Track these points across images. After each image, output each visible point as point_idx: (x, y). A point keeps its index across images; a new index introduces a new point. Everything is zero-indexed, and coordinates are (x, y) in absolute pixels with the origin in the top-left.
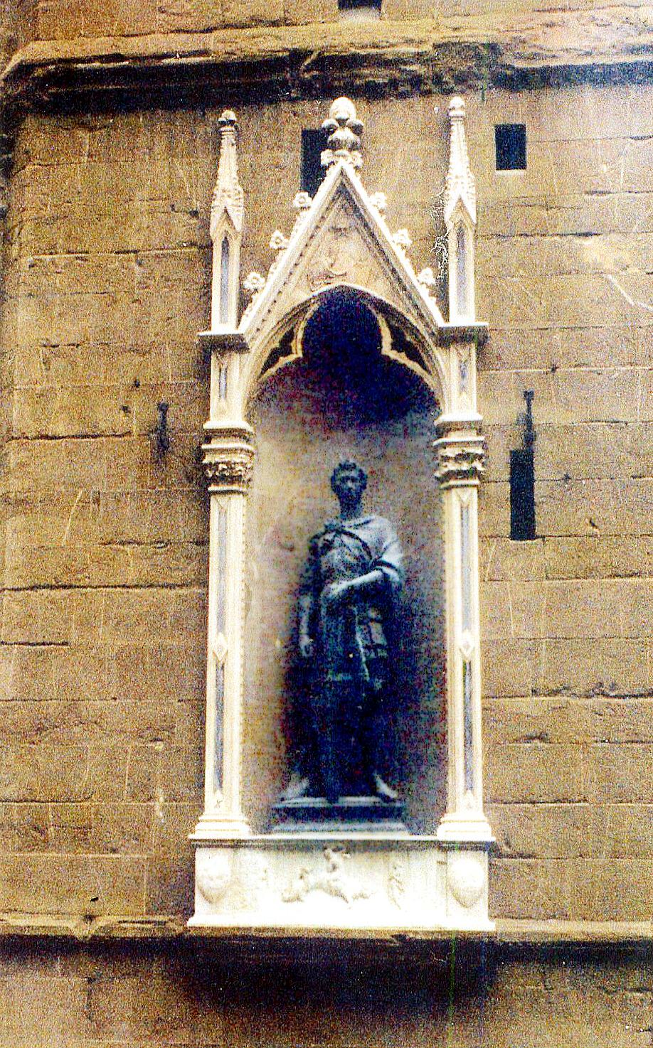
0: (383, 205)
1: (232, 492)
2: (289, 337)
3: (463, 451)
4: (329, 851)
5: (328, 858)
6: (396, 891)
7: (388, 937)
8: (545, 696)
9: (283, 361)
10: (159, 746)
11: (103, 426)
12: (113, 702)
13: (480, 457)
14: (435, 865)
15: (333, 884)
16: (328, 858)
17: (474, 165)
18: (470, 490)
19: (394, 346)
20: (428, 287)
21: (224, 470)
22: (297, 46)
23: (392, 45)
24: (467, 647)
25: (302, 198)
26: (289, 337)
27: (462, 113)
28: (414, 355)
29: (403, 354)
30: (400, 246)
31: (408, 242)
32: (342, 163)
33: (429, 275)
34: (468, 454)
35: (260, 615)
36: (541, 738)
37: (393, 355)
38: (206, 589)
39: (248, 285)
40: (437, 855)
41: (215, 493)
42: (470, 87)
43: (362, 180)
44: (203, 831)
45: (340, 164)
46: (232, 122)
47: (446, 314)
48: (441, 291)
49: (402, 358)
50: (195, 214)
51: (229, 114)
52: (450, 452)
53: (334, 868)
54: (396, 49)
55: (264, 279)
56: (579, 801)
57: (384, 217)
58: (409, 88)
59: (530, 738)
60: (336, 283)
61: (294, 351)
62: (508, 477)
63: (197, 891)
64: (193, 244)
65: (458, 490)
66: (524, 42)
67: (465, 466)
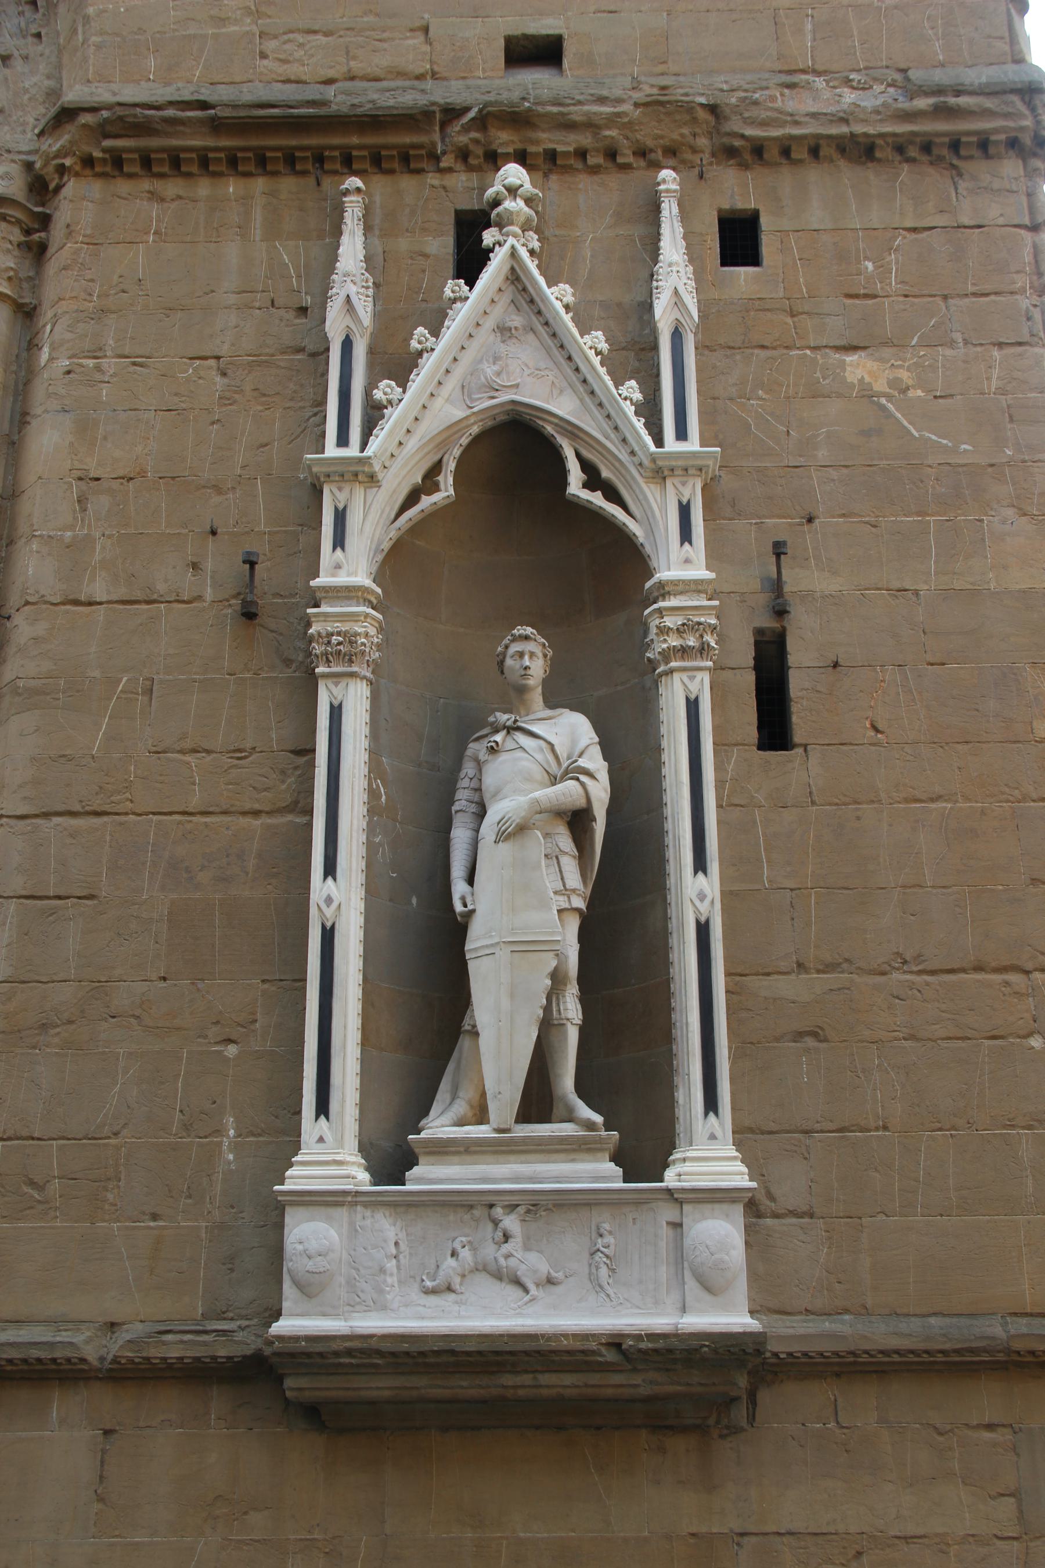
0: (569, 299)
1: (353, 675)
2: (436, 468)
3: (689, 620)
4: (498, 1211)
5: (496, 1223)
6: (604, 1271)
7: (593, 1345)
8: (818, 972)
9: (426, 502)
10: (232, 1050)
11: (161, 587)
12: (162, 984)
13: (713, 629)
15: (502, 1261)
16: (496, 1223)
17: (693, 256)
19: (586, 486)
20: (632, 404)
21: (340, 643)
22: (448, 100)
23: (580, 103)
24: (702, 897)
25: (453, 287)
26: (436, 468)
27: (674, 187)
28: (613, 495)
29: (599, 493)
30: (593, 351)
31: (604, 346)
32: (511, 241)
33: (632, 389)
34: (699, 624)
35: (650, 143)
36: (814, 1034)
37: (585, 495)
38: (308, 818)
39: (378, 395)
40: (668, 1212)
41: (325, 676)
42: (683, 162)
43: (539, 267)
44: (298, 1178)
45: (507, 247)
46: (358, 190)
47: (659, 442)
48: (650, 410)
49: (597, 499)
50: (303, 311)
51: (355, 182)
52: (670, 621)
54: (586, 108)
55: (400, 390)
56: (877, 1129)
57: (571, 314)
58: (600, 160)
60: (504, 397)
61: (442, 486)
62: (752, 663)
63: (286, 1277)
64: (301, 350)
65: (684, 676)
66: (756, 103)
67: (692, 641)
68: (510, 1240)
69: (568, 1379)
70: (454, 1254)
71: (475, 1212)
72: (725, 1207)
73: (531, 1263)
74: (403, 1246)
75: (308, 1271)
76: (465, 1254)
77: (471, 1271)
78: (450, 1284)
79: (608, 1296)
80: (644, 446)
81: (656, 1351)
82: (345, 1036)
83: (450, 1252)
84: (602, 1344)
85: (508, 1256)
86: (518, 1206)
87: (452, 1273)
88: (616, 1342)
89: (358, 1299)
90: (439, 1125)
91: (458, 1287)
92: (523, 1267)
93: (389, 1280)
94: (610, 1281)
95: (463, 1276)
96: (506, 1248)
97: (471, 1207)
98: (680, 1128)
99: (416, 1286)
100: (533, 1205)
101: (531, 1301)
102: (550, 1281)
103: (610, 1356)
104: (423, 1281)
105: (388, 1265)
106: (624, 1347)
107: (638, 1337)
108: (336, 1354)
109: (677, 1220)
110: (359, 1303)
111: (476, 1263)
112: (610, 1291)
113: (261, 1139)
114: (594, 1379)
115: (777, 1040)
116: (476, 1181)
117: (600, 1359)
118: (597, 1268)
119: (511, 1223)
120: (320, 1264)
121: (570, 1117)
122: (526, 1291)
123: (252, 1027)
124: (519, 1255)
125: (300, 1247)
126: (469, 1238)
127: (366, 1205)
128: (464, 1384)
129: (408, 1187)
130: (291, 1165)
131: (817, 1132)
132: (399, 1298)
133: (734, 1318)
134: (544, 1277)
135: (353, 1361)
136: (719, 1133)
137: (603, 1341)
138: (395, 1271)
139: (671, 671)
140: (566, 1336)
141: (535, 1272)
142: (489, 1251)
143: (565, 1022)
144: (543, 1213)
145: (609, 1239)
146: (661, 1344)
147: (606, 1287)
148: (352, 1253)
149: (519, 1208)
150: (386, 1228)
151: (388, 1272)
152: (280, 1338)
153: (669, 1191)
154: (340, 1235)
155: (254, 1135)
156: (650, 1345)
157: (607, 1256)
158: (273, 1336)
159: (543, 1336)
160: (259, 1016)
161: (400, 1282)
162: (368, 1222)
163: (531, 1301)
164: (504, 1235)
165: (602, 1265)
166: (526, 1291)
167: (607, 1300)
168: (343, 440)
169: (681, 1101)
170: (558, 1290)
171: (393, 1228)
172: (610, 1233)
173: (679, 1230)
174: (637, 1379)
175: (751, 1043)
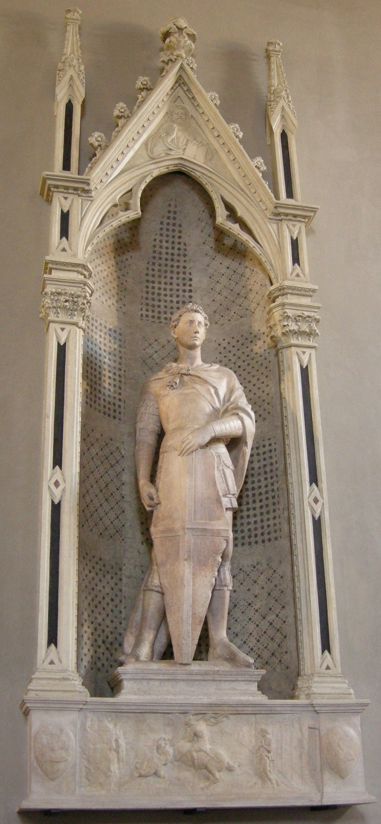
18: (308, 351)
34: (309, 317)
39: (92, 140)
52: (290, 312)
65: (299, 350)
67: (305, 327)
80: (270, 199)
139: (290, 346)
168: (67, 166)
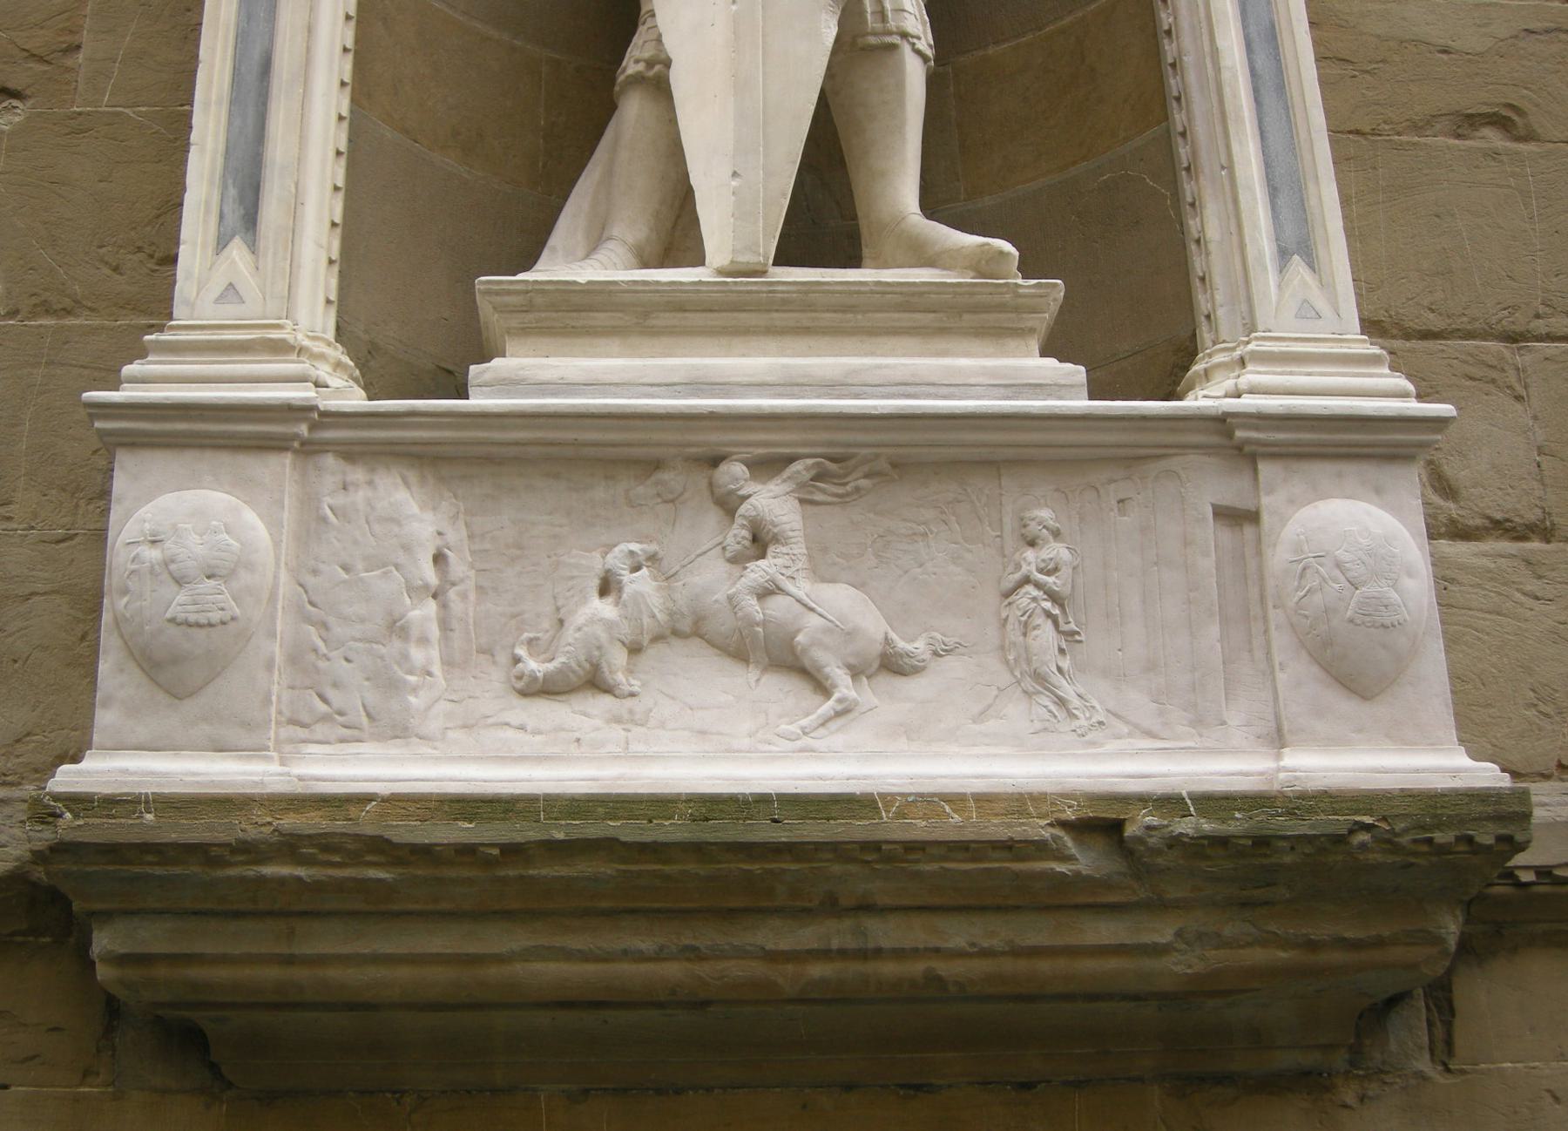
5: (728, 505)
6: (1046, 635)
7: (1039, 829)
14: (1208, 532)
15: (752, 605)
16: (728, 505)
36: (1500, 122)
40: (1216, 485)
53: (760, 541)
59: (1469, 122)
63: (109, 641)
68: (771, 550)
69: (958, 933)
70: (607, 586)
71: (665, 476)
72: (1371, 471)
73: (835, 609)
74: (458, 565)
75: (172, 620)
76: (640, 584)
77: (658, 638)
78: (596, 668)
79: (1061, 702)
81: (1222, 841)
82: (308, 50)
83: (596, 582)
84: (1064, 824)
85: (766, 592)
86: (791, 459)
87: (603, 636)
88: (1102, 822)
89: (322, 708)
90: (563, 265)
91: (620, 677)
92: (814, 621)
93: (417, 655)
94: (1066, 664)
95: (635, 650)
96: (760, 570)
97: (657, 465)
98: (1217, 300)
99: (496, 677)
100: (833, 459)
101: (838, 714)
102: (892, 665)
103: (1085, 860)
104: (517, 660)
105: (415, 614)
106: (1130, 830)
107: (1170, 803)
108: (249, 851)
109: (1246, 504)
110: (325, 718)
111: (671, 614)
112: (1068, 690)
113: (70, 321)
114: (1037, 932)
115: (1417, 127)
116: (670, 387)
117: (1061, 868)
118: (1026, 628)
119: (770, 500)
120: (216, 599)
121: (921, 255)
122: (822, 687)
123: (69, 62)
124: (802, 587)
125: (152, 554)
126: (652, 548)
127: (351, 453)
128: (645, 944)
129: (477, 401)
130: (141, 353)
131: (1539, 339)
132: (443, 706)
133: (1417, 755)
134: (878, 648)
135: (301, 872)
136: (1321, 304)
137: (1070, 815)
138: (434, 631)
140: (956, 800)
141: (850, 634)
142: (713, 580)
143: (896, 40)
144: (864, 483)
145: (1056, 551)
146: (1237, 825)
147: (1057, 679)
148: (310, 580)
149: (797, 466)
150: (412, 513)
151: (415, 632)
152: (79, 802)
153: (1222, 422)
154: (274, 525)
155: (47, 309)
156: (1207, 826)
157: (1053, 596)
158: (57, 797)
159: (888, 798)
160: (85, 37)
161: (448, 663)
162: (359, 496)
163: (838, 714)
164: (755, 539)
165: (1039, 620)
166: (822, 687)
167: (1061, 714)
169: (1213, 232)
170: (914, 687)
171: (429, 516)
172: (1056, 534)
173: (1249, 531)
174: (1162, 931)
175: (1358, 132)
